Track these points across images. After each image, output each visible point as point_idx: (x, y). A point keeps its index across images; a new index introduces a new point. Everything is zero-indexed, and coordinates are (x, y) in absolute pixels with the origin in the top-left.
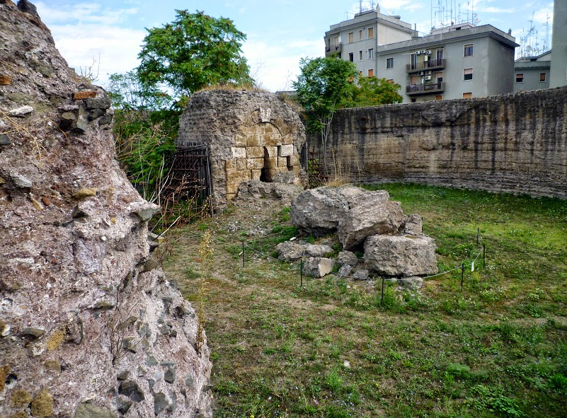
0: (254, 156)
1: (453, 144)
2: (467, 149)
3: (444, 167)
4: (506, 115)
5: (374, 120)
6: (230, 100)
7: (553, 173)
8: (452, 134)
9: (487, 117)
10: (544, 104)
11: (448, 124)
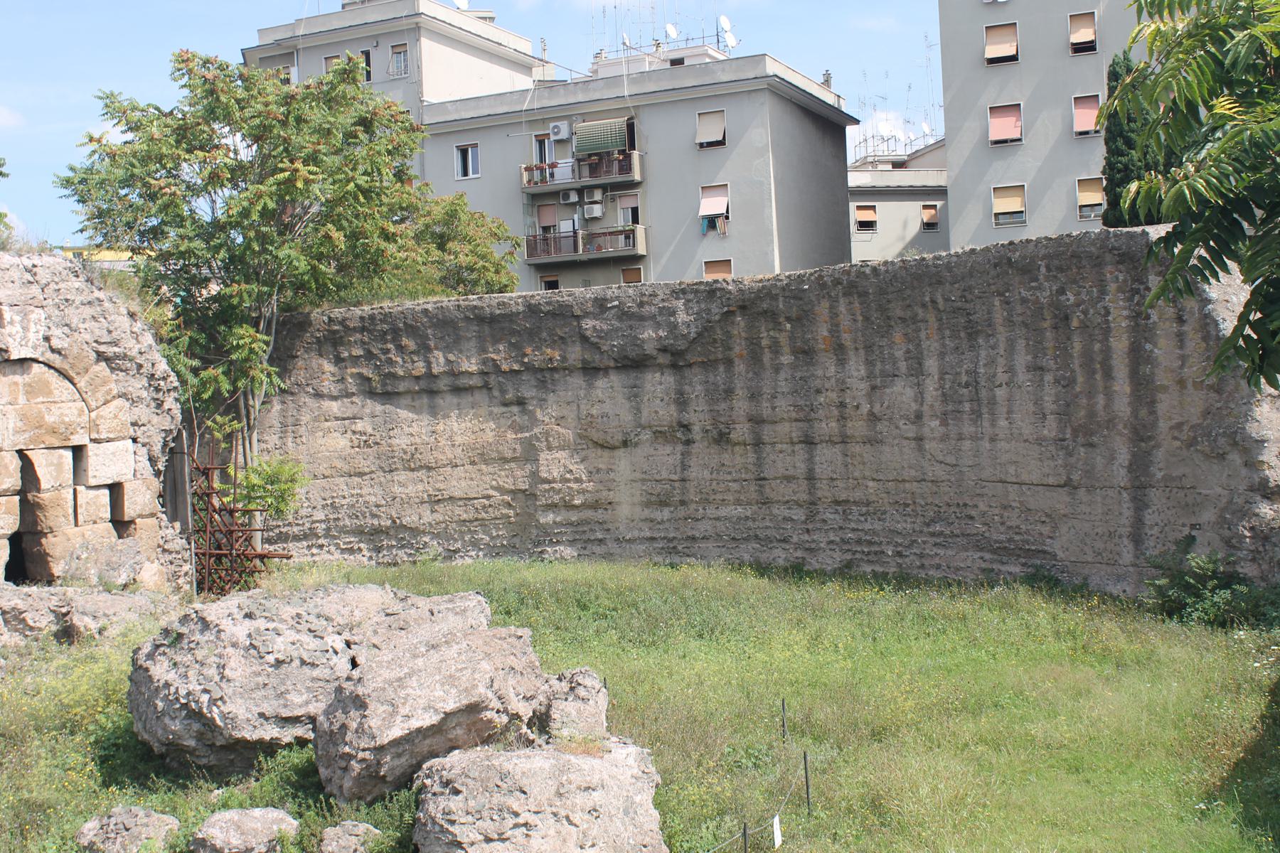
1: (686, 427)
2: (728, 441)
3: (663, 504)
4: (835, 329)
5: (424, 349)
7: (982, 507)
8: (680, 393)
9: (783, 339)
10: (940, 300)
11: (663, 359)
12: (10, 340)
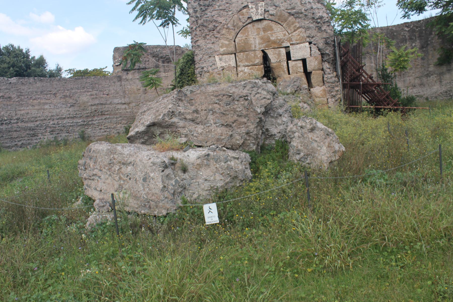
0: (247, 64)
6: (207, 3)
12: (252, 14)
